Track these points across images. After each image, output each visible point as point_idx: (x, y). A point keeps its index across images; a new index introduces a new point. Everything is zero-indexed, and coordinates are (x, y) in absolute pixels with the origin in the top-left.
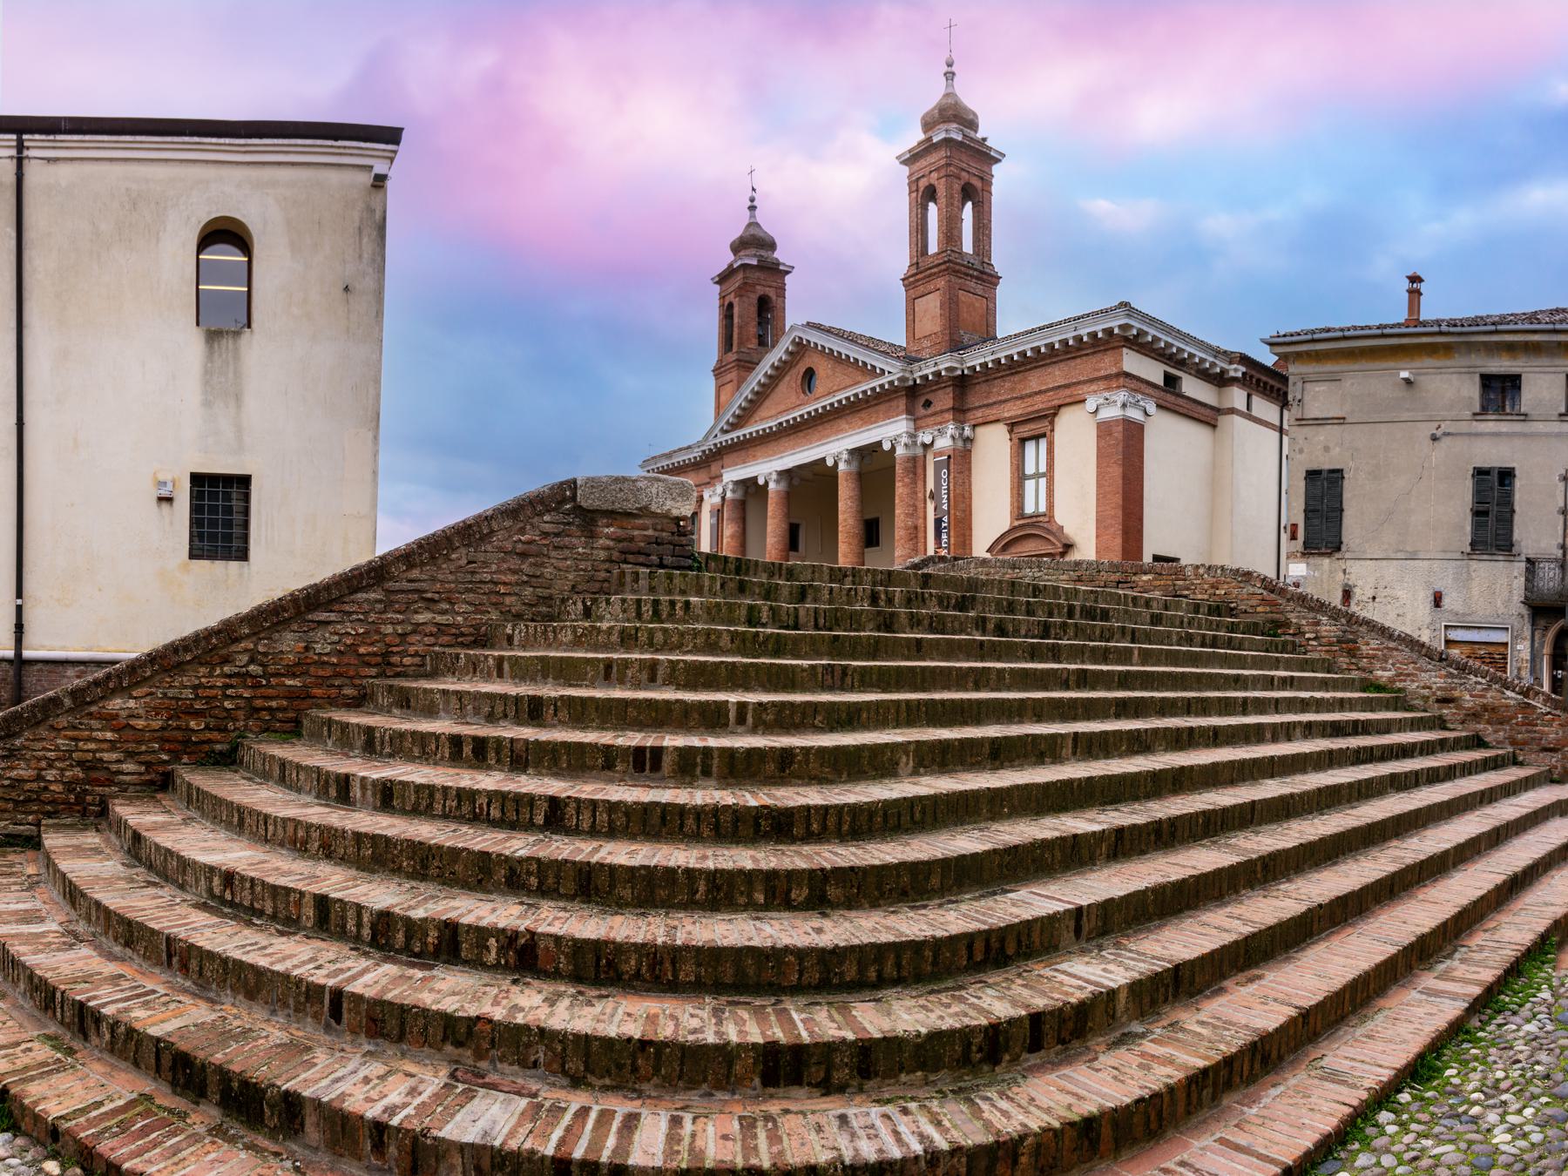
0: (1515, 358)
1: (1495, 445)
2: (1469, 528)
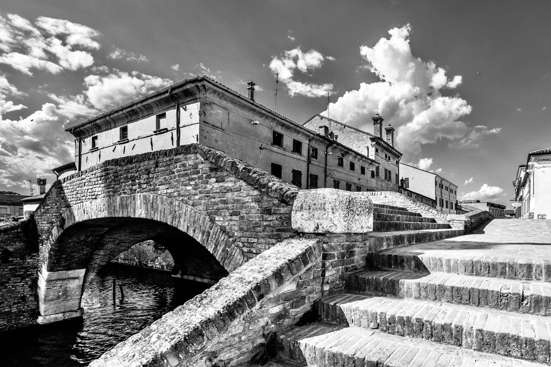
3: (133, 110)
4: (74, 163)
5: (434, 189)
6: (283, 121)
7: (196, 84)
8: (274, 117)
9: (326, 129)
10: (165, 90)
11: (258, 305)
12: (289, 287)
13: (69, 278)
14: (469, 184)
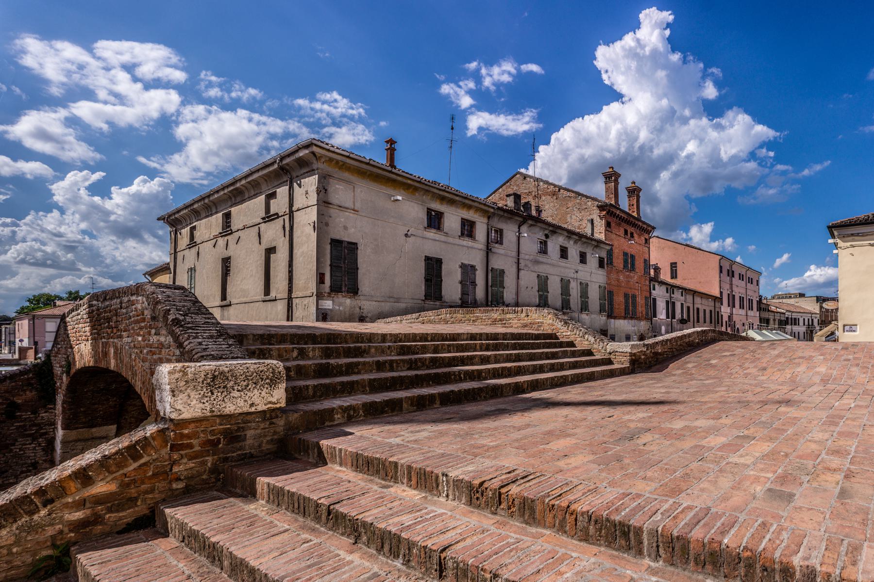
0: (442, 204)
1: (432, 243)
3: (236, 189)
4: (168, 264)
5: (718, 279)
6: (441, 193)
7: (311, 149)
8: (427, 188)
9: (517, 197)
10: (272, 160)
11: (43, 512)
12: (102, 487)
13: (93, 438)
14: (783, 265)
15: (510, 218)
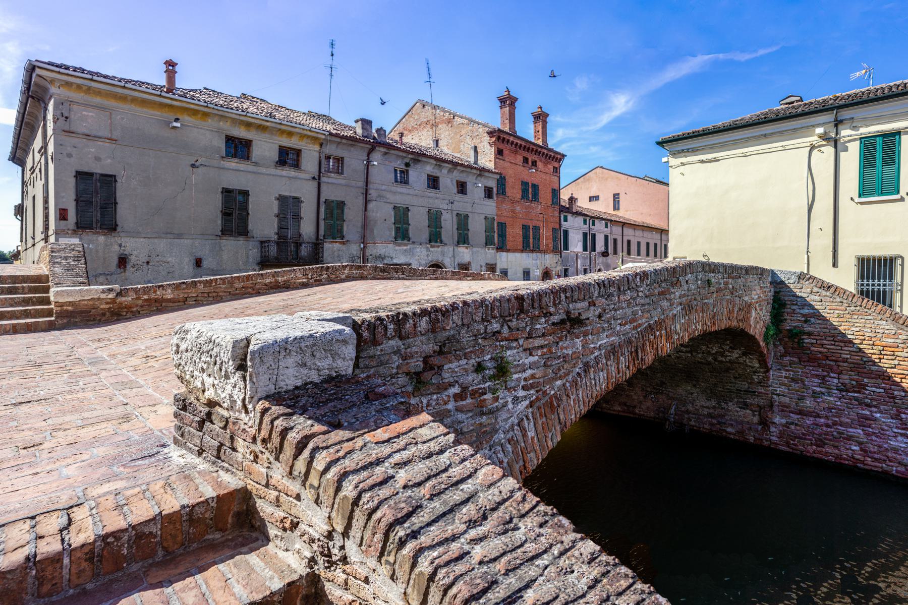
2: (219, 222)
15: (352, 145)
